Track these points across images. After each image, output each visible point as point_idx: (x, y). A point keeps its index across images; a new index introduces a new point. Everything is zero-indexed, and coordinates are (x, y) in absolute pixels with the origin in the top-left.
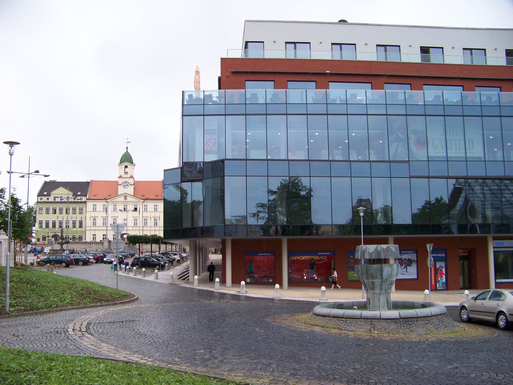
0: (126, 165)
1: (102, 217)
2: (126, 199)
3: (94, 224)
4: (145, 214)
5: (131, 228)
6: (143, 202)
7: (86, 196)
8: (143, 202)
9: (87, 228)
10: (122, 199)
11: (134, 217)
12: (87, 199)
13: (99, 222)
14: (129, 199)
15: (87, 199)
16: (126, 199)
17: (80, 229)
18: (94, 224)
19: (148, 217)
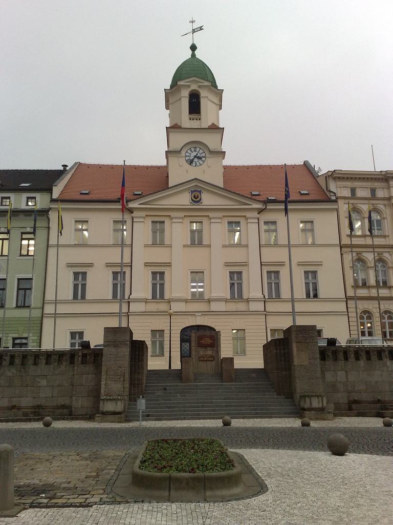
0: (194, 87)
1: (108, 265)
2: (196, 199)
3: (79, 293)
4: (271, 255)
5: (221, 306)
6: (260, 211)
7: (50, 191)
8: (260, 211)
9: (49, 309)
10: (184, 199)
11: (227, 264)
12: (53, 201)
13: (99, 284)
14: (208, 200)
15: (53, 201)
16: (196, 199)
17: (24, 313)
18: (79, 293)
19: (281, 264)
